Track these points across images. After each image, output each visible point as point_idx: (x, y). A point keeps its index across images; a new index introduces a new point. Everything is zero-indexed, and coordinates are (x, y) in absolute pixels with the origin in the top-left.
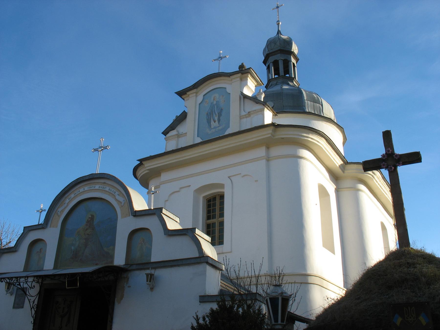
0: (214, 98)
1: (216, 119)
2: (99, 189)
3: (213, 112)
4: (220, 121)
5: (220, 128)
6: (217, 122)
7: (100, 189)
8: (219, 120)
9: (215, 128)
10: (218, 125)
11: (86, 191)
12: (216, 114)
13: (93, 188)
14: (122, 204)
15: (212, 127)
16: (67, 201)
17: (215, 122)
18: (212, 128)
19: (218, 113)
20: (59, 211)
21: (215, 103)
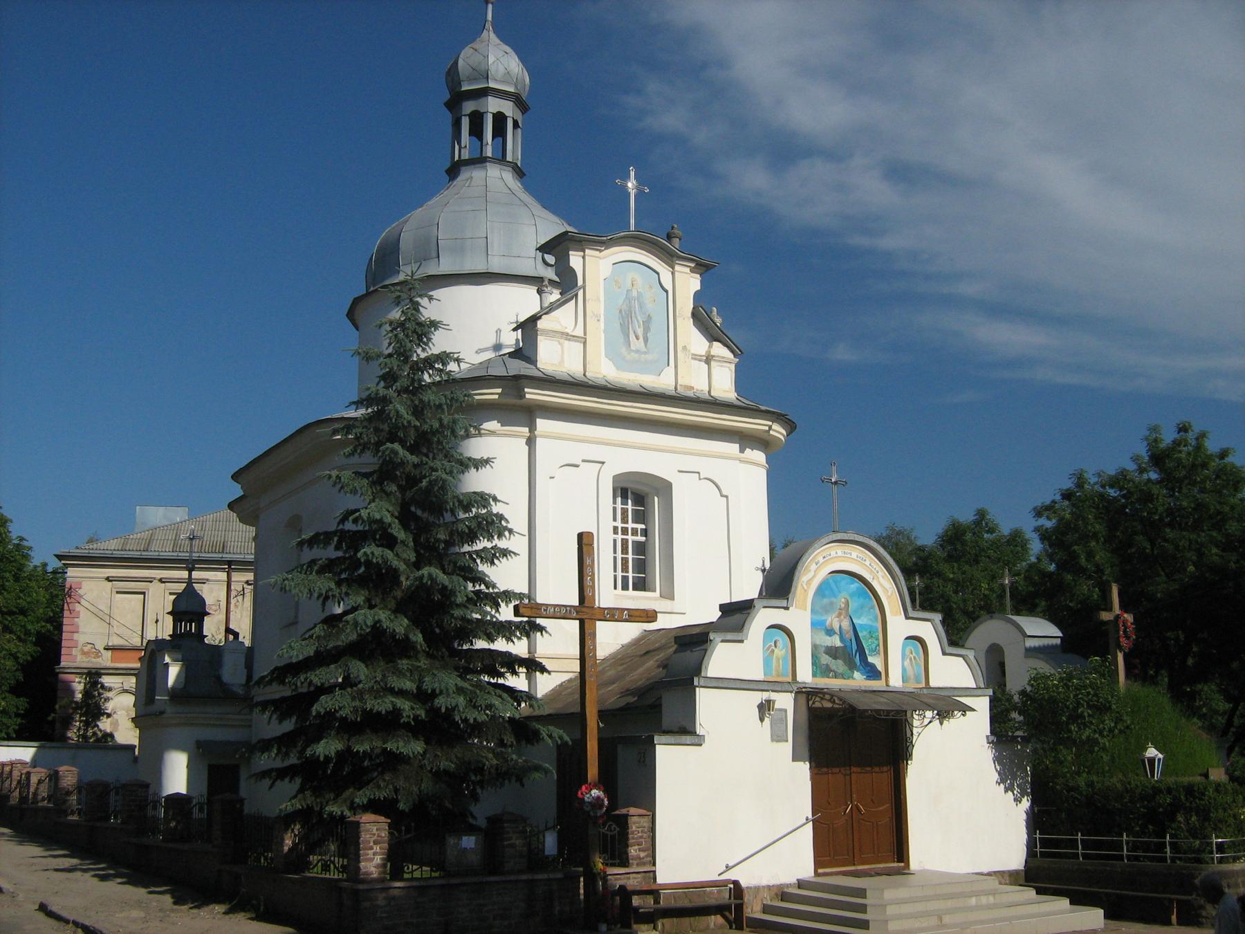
0: (632, 281)
1: (640, 332)
2: (857, 560)
3: (633, 315)
4: (648, 340)
5: (649, 357)
6: (641, 339)
7: (858, 559)
8: (646, 340)
9: (637, 351)
10: (644, 349)
11: (839, 557)
12: (638, 321)
13: (849, 556)
14: (889, 594)
15: (633, 347)
16: (813, 567)
17: (637, 338)
18: (633, 351)
19: (643, 322)
20: (803, 582)
21: (635, 294)
